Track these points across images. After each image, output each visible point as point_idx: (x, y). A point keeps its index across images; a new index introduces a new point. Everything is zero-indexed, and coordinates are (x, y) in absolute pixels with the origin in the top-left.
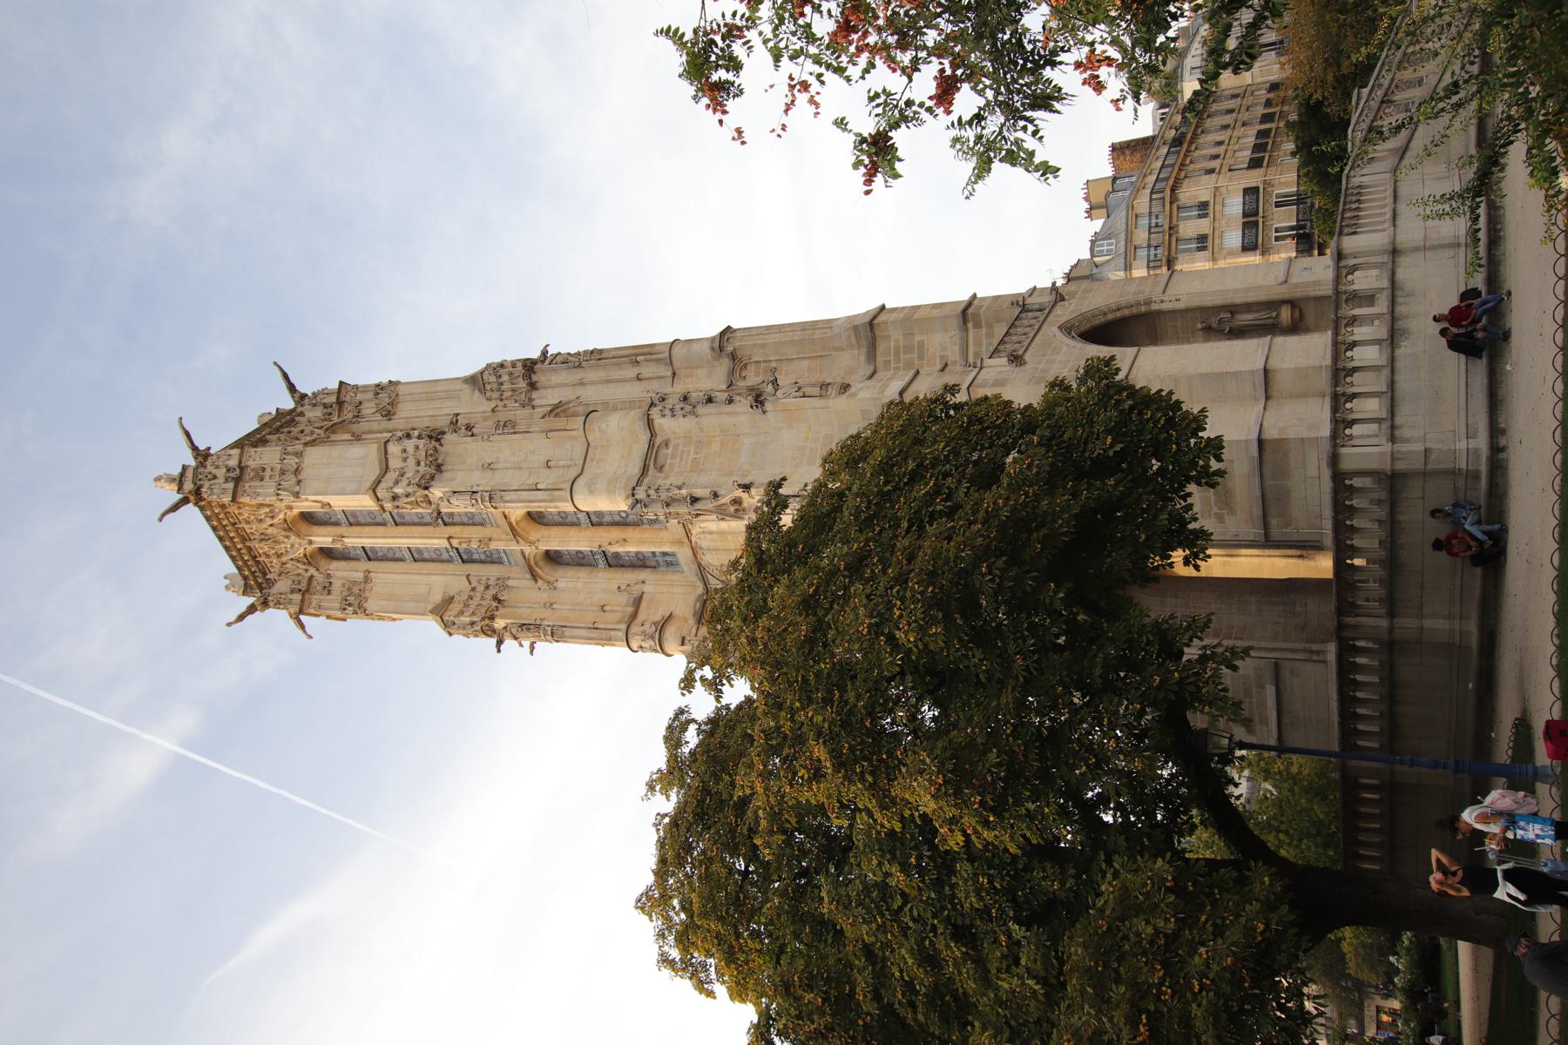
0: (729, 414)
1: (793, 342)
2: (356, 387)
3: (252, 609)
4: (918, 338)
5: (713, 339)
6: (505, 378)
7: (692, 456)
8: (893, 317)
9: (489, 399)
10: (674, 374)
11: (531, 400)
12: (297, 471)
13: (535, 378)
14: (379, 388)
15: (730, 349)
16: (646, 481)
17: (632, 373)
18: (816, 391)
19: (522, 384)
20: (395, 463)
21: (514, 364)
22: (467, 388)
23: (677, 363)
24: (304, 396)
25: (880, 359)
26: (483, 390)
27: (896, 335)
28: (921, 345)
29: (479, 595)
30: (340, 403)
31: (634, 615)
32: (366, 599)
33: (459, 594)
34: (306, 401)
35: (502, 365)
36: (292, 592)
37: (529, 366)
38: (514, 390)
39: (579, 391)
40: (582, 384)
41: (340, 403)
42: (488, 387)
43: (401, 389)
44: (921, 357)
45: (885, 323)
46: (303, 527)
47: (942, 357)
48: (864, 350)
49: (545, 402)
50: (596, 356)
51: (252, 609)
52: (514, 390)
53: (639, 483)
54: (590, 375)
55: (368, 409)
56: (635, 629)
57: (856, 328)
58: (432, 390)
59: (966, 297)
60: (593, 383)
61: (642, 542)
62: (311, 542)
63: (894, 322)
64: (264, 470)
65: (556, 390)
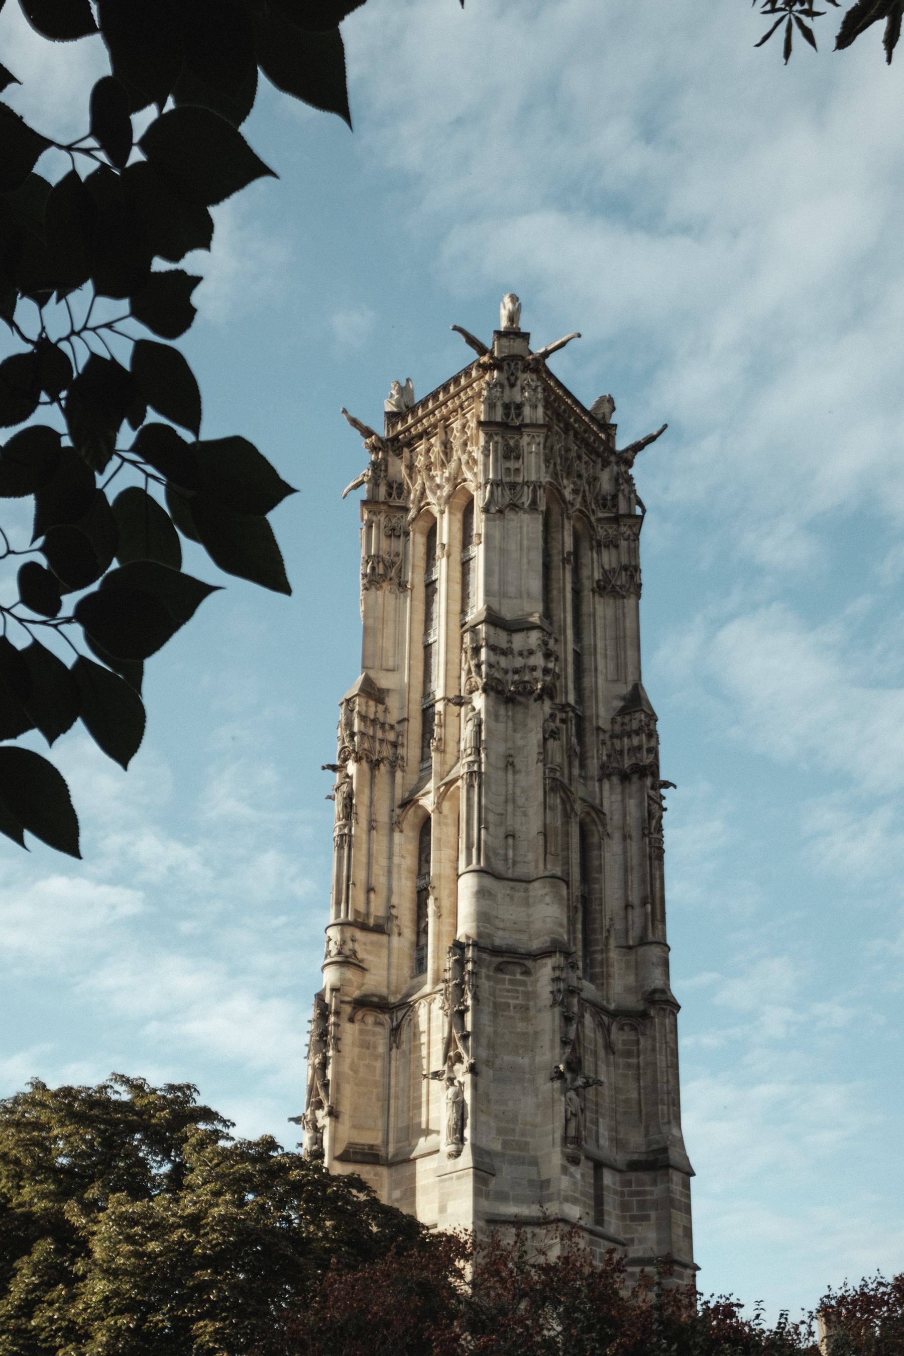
0: (552, 1041)
1: (655, 1081)
2: (636, 537)
3: (367, 432)
4: (653, 1214)
5: (665, 990)
6: (636, 741)
7: (512, 1002)
8: (677, 1187)
9: (613, 721)
10: (630, 948)
11: (609, 776)
13: (635, 778)
14: (633, 570)
15: (652, 1013)
16: (485, 956)
17: (635, 897)
19: (627, 763)
21: (654, 751)
22: (625, 689)
23: (641, 950)
24: (630, 464)
25: (633, 1176)
26: (623, 712)
27: (656, 1192)
28: (646, 1218)
30: (617, 519)
31: (364, 927)
34: (623, 468)
35: (652, 735)
36: (390, 486)
37: (653, 769)
38: (621, 752)
39: (617, 835)
40: (625, 837)
41: (617, 519)
42: (627, 719)
43: (631, 602)
44: (633, 1218)
45: (670, 1180)
46: (461, 501)
47: (632, 1240)
48: (643, 1157)
49: (606, 793)
50: (655, 854)
51: (367, 432)
52: (621, 752)
54: (634, 847)
55: (608, 558)
56: (349, 931)
57: (665, 1150)
58: (628, 643)
59: (697, 1260)
60: (625, 852)
61: (438, 936)
62: (442, 512)
63: (669, 1191)
65: (617, 806)
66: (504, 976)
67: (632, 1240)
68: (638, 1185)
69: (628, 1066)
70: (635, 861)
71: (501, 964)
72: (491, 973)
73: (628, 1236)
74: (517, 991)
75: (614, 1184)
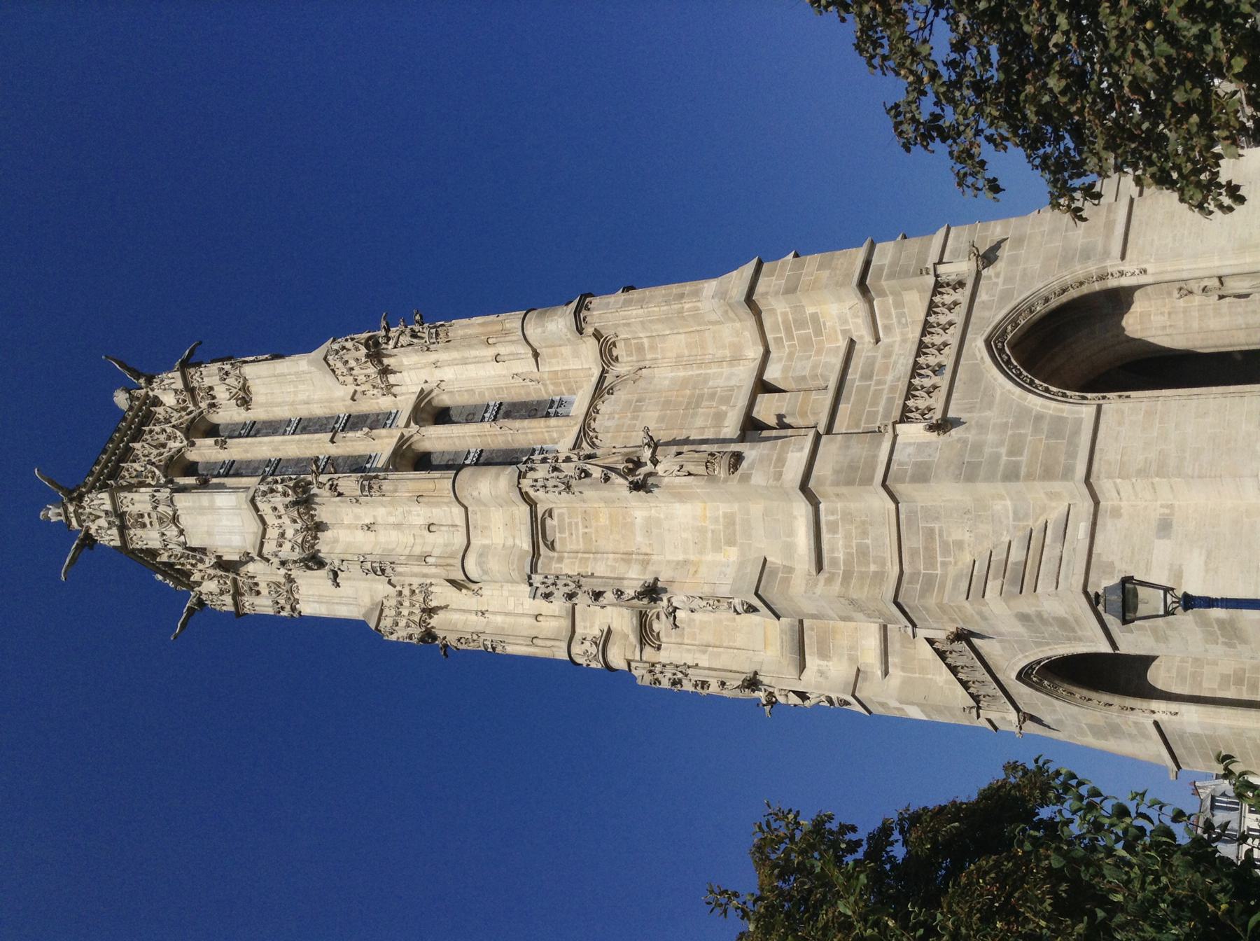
10: (536, 355)
12: (175, 519)
18: (701, 469)
19: (372, 370)
20: (271, 519)
25: (770, 336)
28: (815, 318)
29: (406, 603)
32: (297, 601)
33: (387, 597)
39: (438, 375)
44: (818, 332)
47: (844, 332)
53: (534, 568)
55: (221, 394)
64: (142, 516)
66: (557, 540)
67: (844, 332)
68: (779, 331)
69: (653, 348)
70: (455, 355)
71: (546, 545)
72: (555, 554)
73: (840, 337)
74: (570, 524)
75: (780, 359)
